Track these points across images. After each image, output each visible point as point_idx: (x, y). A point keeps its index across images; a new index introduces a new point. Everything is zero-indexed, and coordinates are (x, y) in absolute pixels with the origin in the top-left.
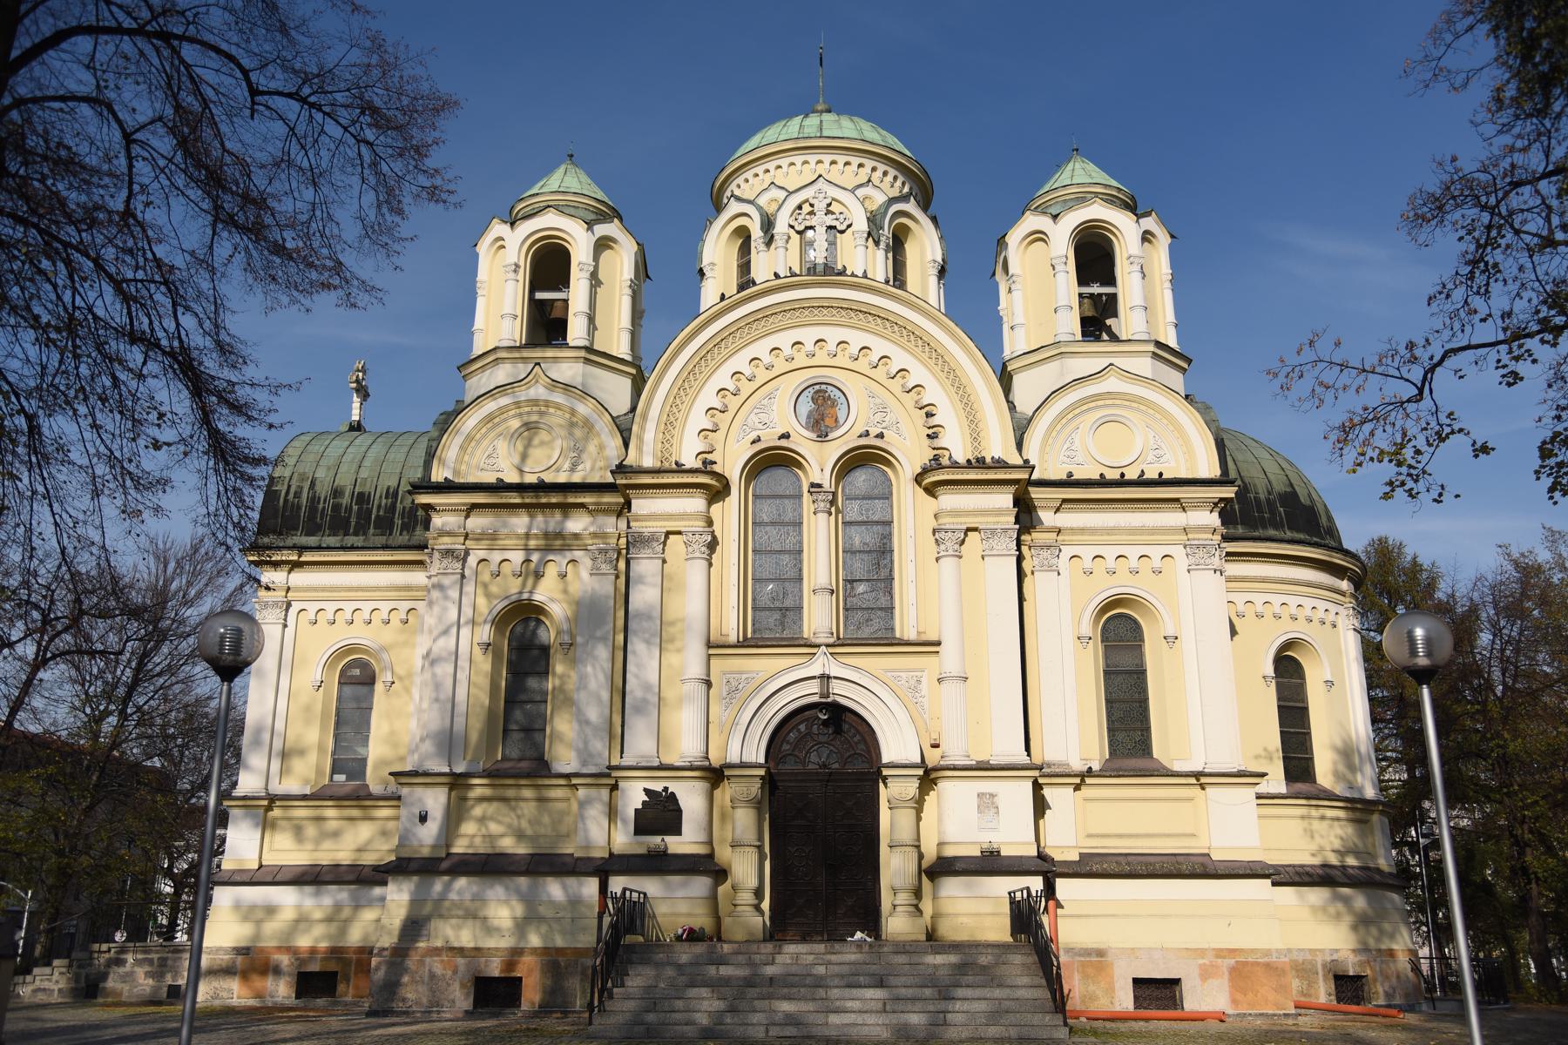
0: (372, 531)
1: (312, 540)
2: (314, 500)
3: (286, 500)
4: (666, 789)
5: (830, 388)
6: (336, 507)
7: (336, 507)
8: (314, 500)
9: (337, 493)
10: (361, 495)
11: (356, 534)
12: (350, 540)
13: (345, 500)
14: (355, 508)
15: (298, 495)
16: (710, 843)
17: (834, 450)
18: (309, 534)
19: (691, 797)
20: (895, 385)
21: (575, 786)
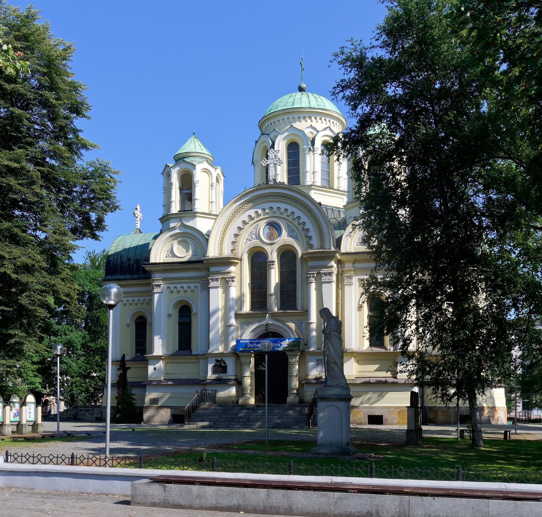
0: (141, 273)
1: (122, 277)
2: (122, 262)
3: (113, 263)
4: (222, 360)
5: (275, 224)
6: (129, 265)
7: (129, 265)
8: (122, 262)
9: (129, 260)
10: (137, 260)
11: (136, 274)
12: (134, 276)
13: (132, 262)
14: (135, 265)
15: (117, 261)
16: (237, 376)
17: (276, 247)
18: (121, 275)
19: (230, 363)
20: (296, 223)
21: (199, 359)
